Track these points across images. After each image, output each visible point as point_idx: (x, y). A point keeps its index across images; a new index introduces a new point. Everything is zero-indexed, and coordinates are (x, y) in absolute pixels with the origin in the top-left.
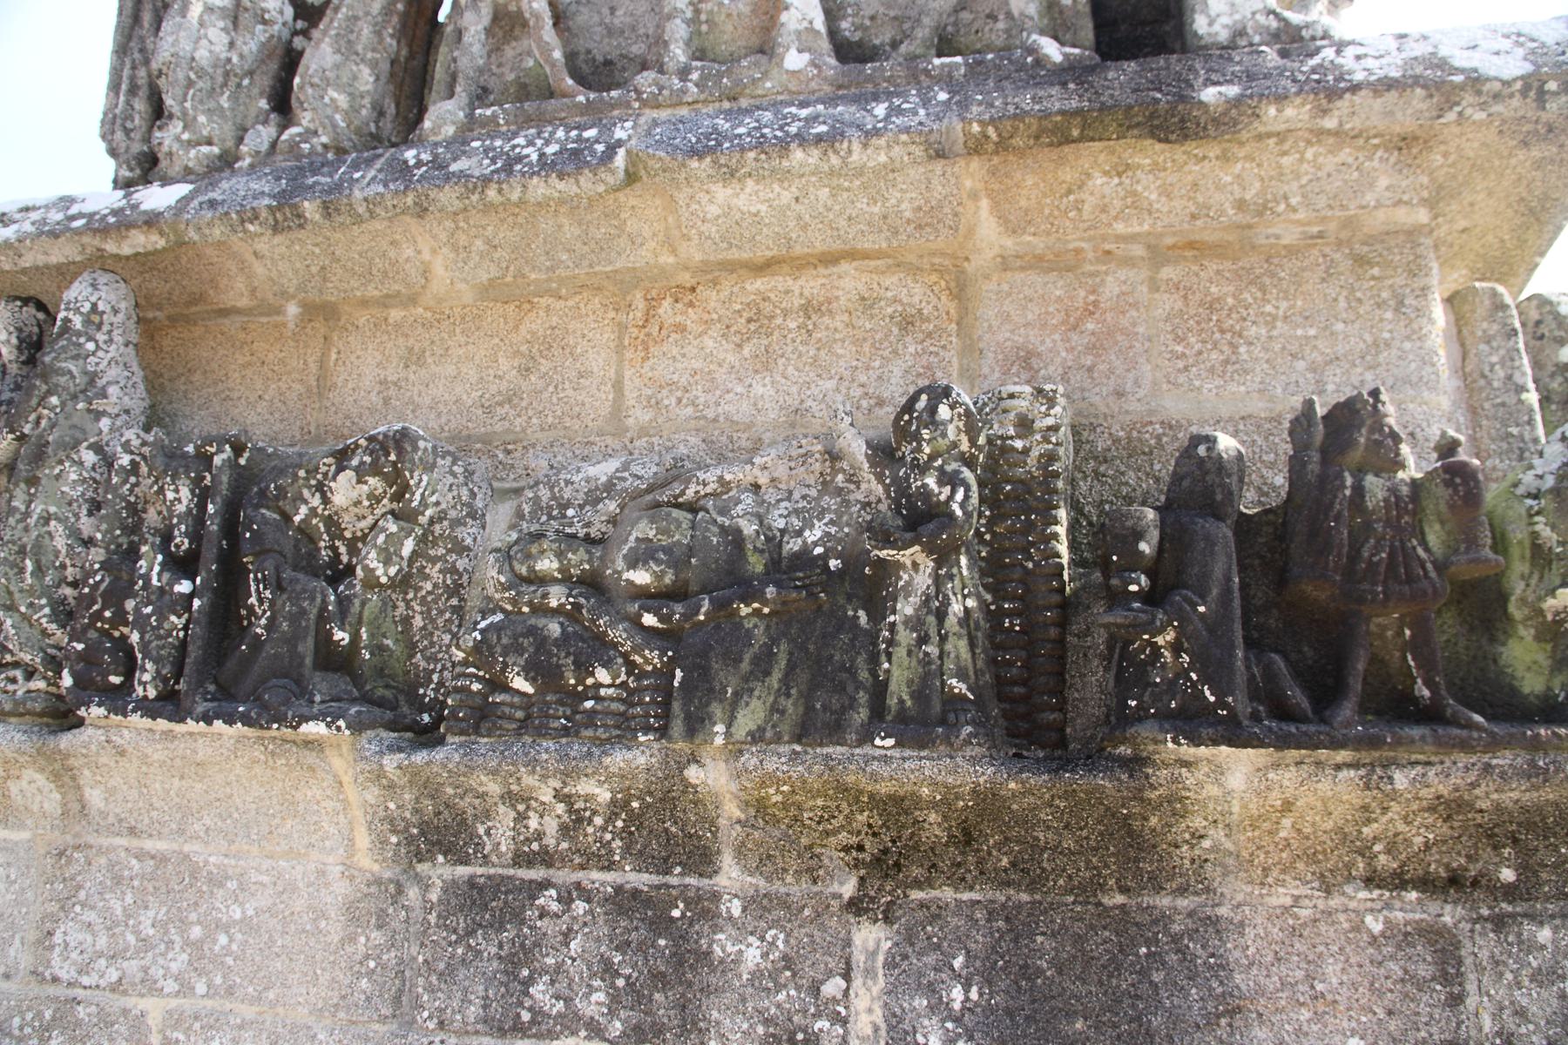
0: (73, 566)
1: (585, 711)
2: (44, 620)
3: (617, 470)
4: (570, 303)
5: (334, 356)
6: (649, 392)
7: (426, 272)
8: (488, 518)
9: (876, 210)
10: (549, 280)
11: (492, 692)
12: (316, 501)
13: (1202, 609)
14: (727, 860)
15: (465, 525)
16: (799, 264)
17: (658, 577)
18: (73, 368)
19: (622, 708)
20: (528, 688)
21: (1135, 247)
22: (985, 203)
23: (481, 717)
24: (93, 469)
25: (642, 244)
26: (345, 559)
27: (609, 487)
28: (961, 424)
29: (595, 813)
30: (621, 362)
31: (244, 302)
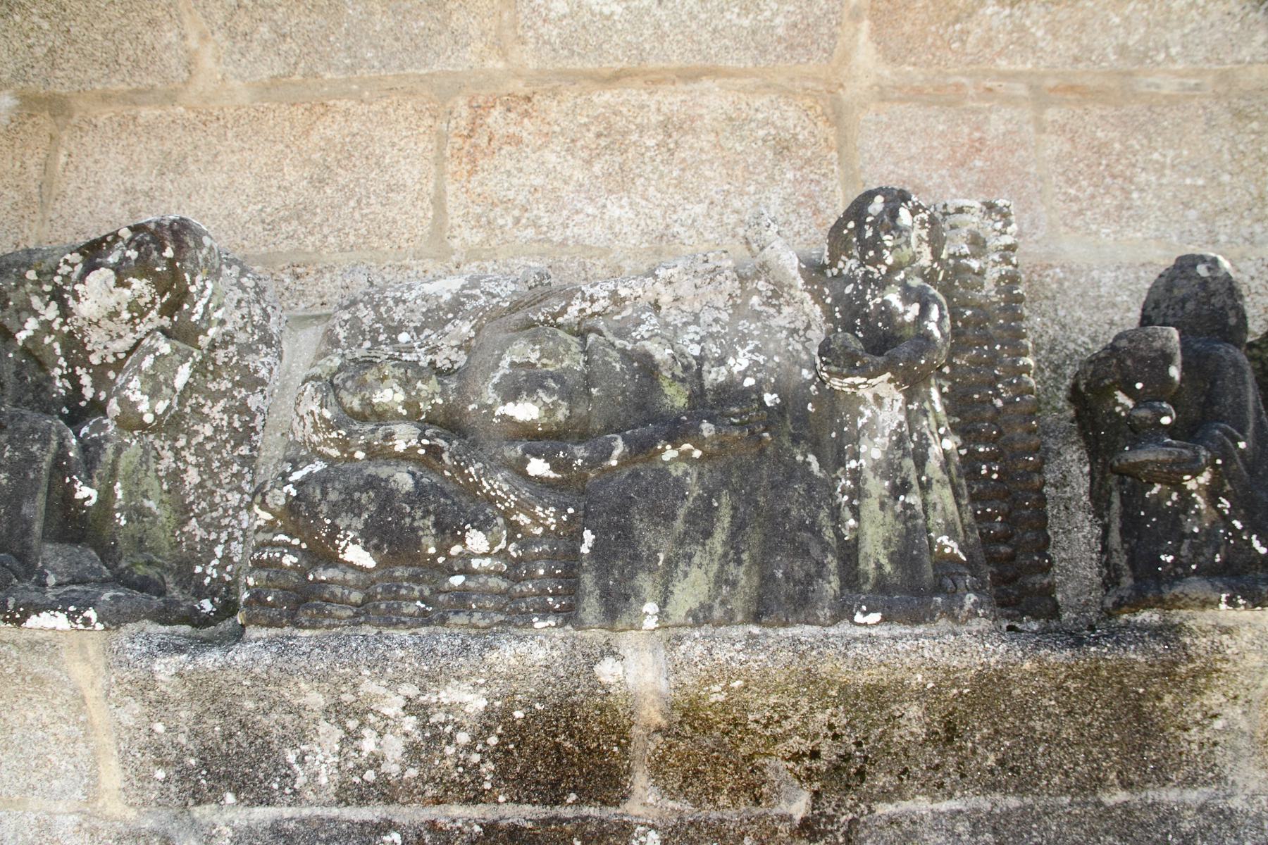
1: (451, 590)
3: (464, 287)
4: (375, 107)
5: (63, 159)
6: (479, 210)
7: (190, 65)
8: (285, 345)
9: (746, 22)
10: (349, 81)
11: (314, 566)
12: (51, 312)
13: (1242, 445)
14: (641, 781)
15: (257, 352)
16: (654, 80)
17: (550, 411)
19: (504, 585)
20: (367, 560)
21: (1018, 86)
22: (865, 25)
23: (299, 602)
25: (467, 45)
26: (88, 393)
27: (456, 306)
28: (924, 233)
29: (459, 727)
30: (441, 175)
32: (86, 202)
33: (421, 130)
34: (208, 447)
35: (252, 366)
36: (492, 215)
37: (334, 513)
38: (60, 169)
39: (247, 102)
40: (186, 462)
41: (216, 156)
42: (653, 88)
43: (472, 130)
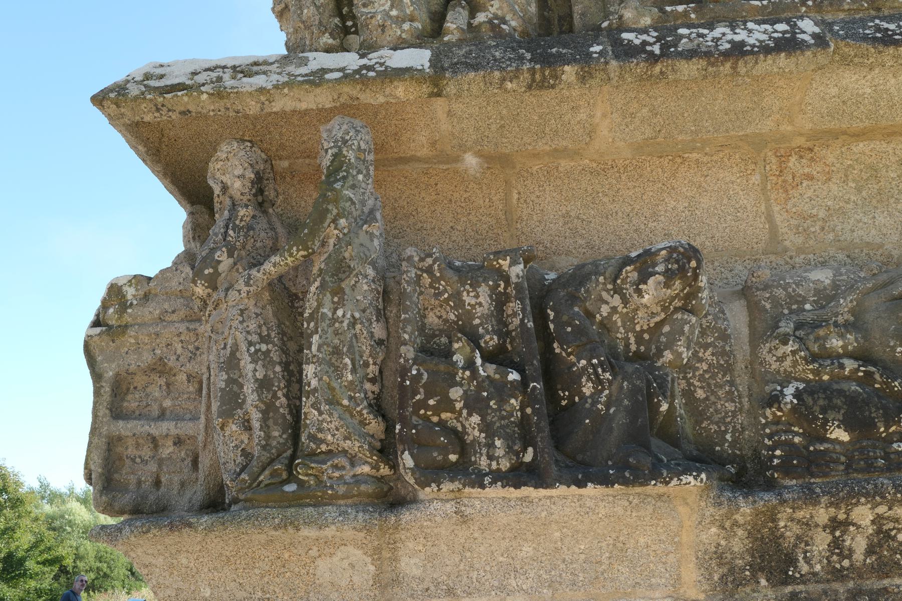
0: (375, 364)
2: (365, 412)
4: (715, 158)
6: (796, 222)
7: (591, 133)
10: (693, 141)
11: (811, 443)
12: (616, 301)
18: (352, 196)
20: (845, 437)
24: (373, 281)
25: (770, 116)
26: (633, 347)
27: (835, 286)
30: (768, 200)
31: (424, 152)
32: (538, 224)
33: (749, 172)
34: (707, 376)
35: (723, 327)
36: (805, 225)
37: (824, 410)
38: (515, 202)
39: (630, 156)
40: (694, 386)
41: (617, 192)
42: (888, 139)
43: (781, 171)
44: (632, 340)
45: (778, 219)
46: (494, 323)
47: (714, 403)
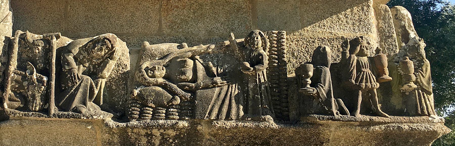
26: (92, 70)
41: (107, 8)
44: (92, 67)
45: (163, 22)
46: (43, 59)
47: (118, 91)
